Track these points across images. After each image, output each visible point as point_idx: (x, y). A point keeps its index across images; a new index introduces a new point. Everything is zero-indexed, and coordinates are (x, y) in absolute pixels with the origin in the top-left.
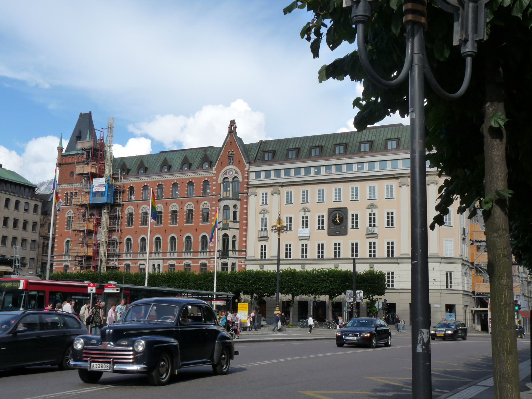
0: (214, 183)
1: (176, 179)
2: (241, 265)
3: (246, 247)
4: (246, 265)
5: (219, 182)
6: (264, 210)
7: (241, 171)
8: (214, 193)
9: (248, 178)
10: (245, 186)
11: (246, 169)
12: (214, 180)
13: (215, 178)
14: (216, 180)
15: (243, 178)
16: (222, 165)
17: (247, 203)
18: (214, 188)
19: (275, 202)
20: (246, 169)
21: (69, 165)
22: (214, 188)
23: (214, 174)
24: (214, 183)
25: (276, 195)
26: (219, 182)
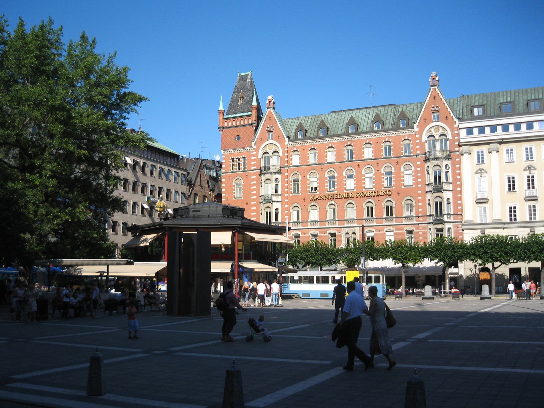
0: (418, 141)
1: (368, 139)
2: (458, 231)
3: (461, 210)
4: (463, 230)
5: (423, 140)
6: (481, 170)
7: (450, 127)
8: (418, 152)
9: (458, 135)
10: (457, 143)
11: (456, 126)
12: (417, 139)
13: (417, 136)
14: (420, 138)
15: (453, 135)
16: (426, 121)
17: (459, 162)
18: (418, 147)
19: (495, 160)
20: (456, 126)
21: (234, 129)
22: (418, 147)
23: (416, 132)
24: (418, 141)
25: (494, 153)
26: (423, 140)
